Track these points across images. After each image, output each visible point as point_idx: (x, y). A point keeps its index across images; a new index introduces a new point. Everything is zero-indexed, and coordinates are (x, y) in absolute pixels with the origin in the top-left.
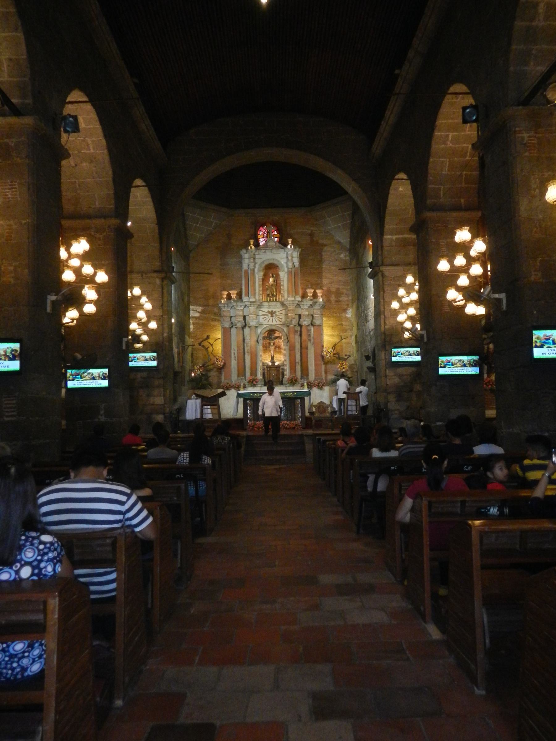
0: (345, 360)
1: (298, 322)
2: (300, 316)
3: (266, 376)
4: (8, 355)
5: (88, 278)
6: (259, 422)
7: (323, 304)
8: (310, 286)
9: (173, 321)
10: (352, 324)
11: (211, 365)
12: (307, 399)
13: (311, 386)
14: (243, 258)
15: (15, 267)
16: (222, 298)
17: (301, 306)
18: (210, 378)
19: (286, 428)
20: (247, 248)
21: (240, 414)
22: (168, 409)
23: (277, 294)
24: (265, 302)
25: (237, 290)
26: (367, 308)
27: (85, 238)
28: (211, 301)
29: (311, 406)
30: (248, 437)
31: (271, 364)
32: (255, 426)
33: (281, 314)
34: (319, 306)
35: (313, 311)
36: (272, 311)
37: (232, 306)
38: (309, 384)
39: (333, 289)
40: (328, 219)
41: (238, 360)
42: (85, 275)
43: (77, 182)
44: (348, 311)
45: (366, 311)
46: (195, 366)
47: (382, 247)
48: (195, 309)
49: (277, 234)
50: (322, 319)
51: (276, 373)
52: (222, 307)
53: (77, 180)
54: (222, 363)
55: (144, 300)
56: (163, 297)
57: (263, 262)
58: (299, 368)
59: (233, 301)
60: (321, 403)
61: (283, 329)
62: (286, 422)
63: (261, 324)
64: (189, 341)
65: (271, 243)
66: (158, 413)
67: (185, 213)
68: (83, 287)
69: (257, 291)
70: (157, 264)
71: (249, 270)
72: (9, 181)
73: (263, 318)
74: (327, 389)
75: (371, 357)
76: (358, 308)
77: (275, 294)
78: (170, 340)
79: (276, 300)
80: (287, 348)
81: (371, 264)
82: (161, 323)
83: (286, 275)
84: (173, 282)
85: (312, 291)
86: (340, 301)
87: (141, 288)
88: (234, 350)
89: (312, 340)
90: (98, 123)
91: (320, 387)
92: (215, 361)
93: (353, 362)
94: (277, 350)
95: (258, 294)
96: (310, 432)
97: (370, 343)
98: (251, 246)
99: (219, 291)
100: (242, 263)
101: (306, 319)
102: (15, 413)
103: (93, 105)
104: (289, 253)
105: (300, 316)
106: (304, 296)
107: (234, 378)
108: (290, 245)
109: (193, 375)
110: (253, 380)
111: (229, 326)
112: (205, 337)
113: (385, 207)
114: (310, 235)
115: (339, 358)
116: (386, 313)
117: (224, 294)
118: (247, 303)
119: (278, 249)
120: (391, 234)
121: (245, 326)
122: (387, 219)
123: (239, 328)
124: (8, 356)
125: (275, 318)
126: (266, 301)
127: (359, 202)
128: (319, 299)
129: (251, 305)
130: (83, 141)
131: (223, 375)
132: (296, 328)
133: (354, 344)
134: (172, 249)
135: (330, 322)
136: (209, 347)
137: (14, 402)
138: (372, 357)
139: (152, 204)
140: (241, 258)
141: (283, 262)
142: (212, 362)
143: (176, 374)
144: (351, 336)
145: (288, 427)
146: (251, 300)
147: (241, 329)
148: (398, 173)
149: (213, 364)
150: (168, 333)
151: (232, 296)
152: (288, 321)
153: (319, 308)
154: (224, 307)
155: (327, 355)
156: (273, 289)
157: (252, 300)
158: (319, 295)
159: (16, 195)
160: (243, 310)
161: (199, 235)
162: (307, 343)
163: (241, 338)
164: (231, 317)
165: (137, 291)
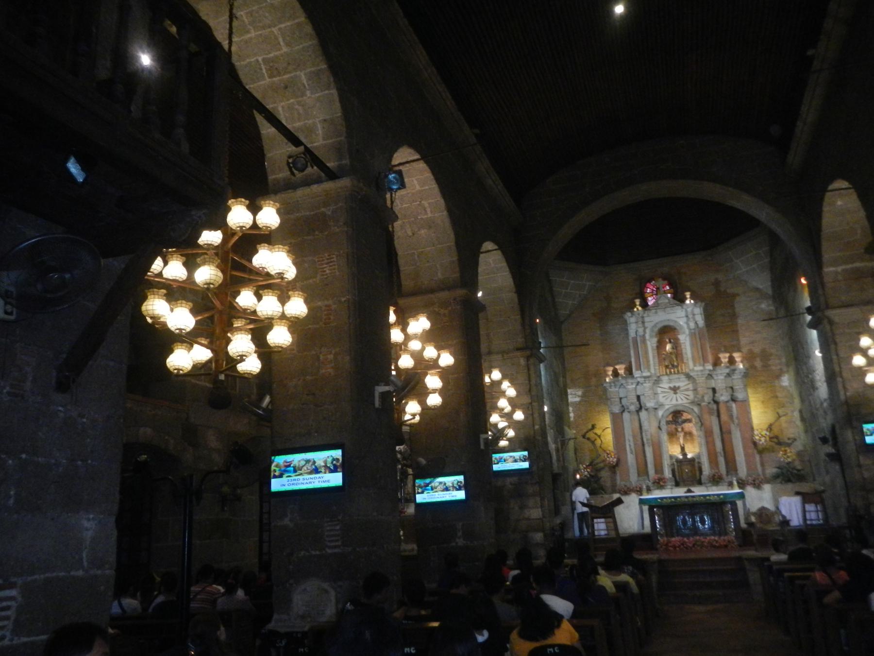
0: (789, 445)
1: (711, 398)
2: (714, 390)
3: (677, 473)
4: (328, 466)
5: (431, 362)
6: (673, 539)
7: (745, 371)
8: (723, 350)
9: (546, 409)
10: (792, 395)
11: (600, 463)
12: (739, 503)
13: (742, 484)
14: (628, 323)
15: (336, 354)
16: (607, 375)
17: (713, 376)
18: (603, 479)
19: (715, 547)
20: (631, 311)
21: (647, 529)
22: (548, 524)
23: (678, 364)
24: (663, 375)
25: (625, 364)
26: (811, 371)
27: (425, 314)
28: (594, 381)
29: (748, 514)
30: (660, 562)
31: (681, 457)
32: (670, 545)
33: (687, 390)
35: (732, 383)
37: (620, 384)
38: (740, 481)
39: (757, 350)
41: (636, 453)
42: (427, 359)
43: (416, 253)
44: (783, 378)
45: (811, 374)
46: (581, 466)
47: (823, 285)
48: (573, 393)
49: (670, 288)
50: (746, 391)
51: (689, 467)
52: (608, 387)
53: (415, 251)
54: (615, 459)
55: (506, 385)
56: (530, 381)
57: (655, 326)
58: (721, 460)
59: (620, 378)
60: (763, 510)
61: (693, 409)
62: (713, 537)
63: (662, 405)
64: (571, 433)
65: (663, 301)
66: (537, 530)
67: (551, 278)
68: (426, 374)
69: (652, 362)
70: (520, 340)
71: (638, 339)
72: (326, 255)
74: (767, 487)
75: (830, 439)
76: (798, 373)
77: (675, 364)
78: (544, 434)
79: (678, 371)
80: (702, 434)
81: (809, 310)
82: (531, 412)
83: (688, 339)
84: (541, 361)
85: (727, 355)
86: (769, 366)
87: (501, 371)
88: (629, 441)
89: (736, 421)
90: (434, 182)
91: (757, 485)
92: (606, 457)
93: (800, 448)
94: (688, 438)
95: (654, 367)
96: (751, 553)
97: (825, 419)
98: (638, 307)
99: (602, 368)
100: (627, 330)
101: (724, 394)
102: (339, 543)
103: (427, 162)
104: (689, 310)
105: (714, 390)
106: (717, 363)
107: (633, 478)
108: (689, 299)
109: (578, 476)
110: (659, 480)
111: (620, 410)
112: (590, 427)
113: (819, 230)
114: (713, 284)
115: (780, 443)
116: (845, 374)
117: (609, 371)
118: (639, 379)
119: (673, 307)
120: (835, 262)
121: (641, 408)
122: (825, 245)
123: (633, 411)
124: (329, 468)
126: (664, 373)
127: (779, 231)
128: (739, 365)
129: (645, 381)
130: (419, 205)
131: (618, 474)
132: (710, 406)
133: (799, 423)
134: (538, 321)
135: (758, 395)
136: (596, 439)
137: (338, 527)
138: (832, 437)
139: (508, 269)
140: (625, 323)
141: (682, 322)
142: (602, 458)
143: (555, 477)
144: (793, 412)
145: (717, 545)
146: (645, 374)
147: (636, 413)
148: (832, 180)
149: (604, 461)
150: (540, 425)
151: (619, 371)
152: (698, 398)
153: (740, 377)
154: (611, 386)
155: (760, 440)
156: (672, 358)
157: (646, 374)
158: (738, 359)
159: (334, 269)
160: (636, 389)
161: (571, 302)
162: (729, 426)
163: (637, 424)
164: (621, 399)
165: (496, 375)
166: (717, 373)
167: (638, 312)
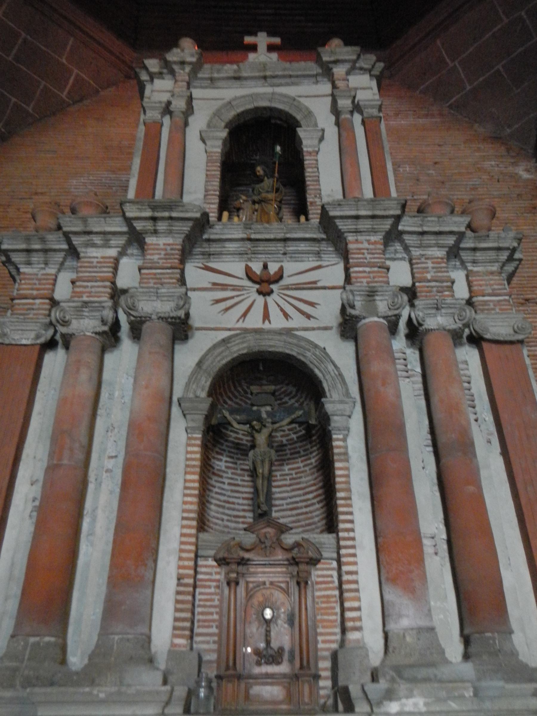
34: (492, 254)
36: (265, 267)
40: (451, 65)
52: (16, 258)
61: (324, 349)
73: (218, 301)
111: (38, 337)
118: (131, 212)
125: (281, 302)
129: (154, 219)
166: (426, 229)
167: (182, 54)
